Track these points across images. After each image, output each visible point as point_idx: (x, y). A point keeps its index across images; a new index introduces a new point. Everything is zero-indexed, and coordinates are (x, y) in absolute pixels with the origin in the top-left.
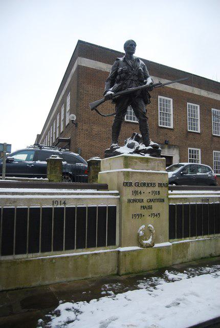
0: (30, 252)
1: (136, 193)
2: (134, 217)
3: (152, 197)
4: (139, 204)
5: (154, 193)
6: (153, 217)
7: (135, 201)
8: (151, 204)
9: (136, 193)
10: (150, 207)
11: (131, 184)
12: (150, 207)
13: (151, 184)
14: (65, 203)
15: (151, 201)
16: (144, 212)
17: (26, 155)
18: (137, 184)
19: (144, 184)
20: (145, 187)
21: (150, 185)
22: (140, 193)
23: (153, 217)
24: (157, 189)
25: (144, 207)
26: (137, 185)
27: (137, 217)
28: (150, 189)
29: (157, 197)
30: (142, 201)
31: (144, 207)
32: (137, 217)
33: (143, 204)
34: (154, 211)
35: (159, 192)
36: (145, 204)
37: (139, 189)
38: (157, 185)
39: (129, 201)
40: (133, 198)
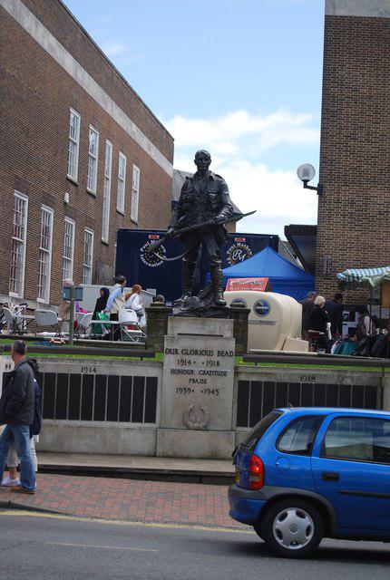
0: (57, 418)
1: (182, 362)
4: (189, 377)
5: (212, 363)
7: (180, 372)
8: (204, 377)
10: (204, 382)
11: (176, 352)
12: (204, 382)
13: (206, 352)
15: (205, 373)
16: (192, 386)
19: (196, 352)
22: (189, 362)
24: (215, 358)
25: (194, 381)
26: (185, 352)
29: (214, 368)
31: (194, 381)
33: (193, 377)
35: (218, 363)
37: (185, 357)
38: (215, 353)
39: (173, 371)
40: (179, 367)
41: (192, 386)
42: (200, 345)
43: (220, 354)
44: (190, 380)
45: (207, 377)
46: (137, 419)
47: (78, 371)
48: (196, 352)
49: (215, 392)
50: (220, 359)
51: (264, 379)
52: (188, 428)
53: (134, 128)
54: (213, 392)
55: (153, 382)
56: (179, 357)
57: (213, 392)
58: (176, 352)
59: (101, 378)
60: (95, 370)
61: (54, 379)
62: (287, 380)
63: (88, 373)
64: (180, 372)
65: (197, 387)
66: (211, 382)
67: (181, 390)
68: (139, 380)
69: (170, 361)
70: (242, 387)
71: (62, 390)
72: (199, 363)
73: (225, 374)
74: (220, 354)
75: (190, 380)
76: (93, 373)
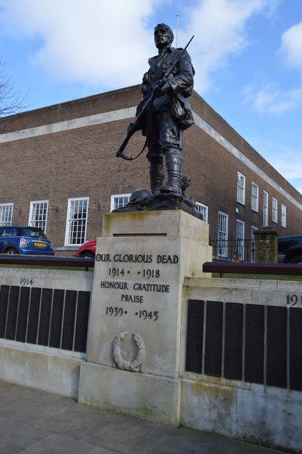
2: (110, 313)
3: (144, 282)
4: (122, 292)
5: (149, 273)
6: (143, 317)
7: (111, 285)
8: (140, 293)
11: (107, 258)
12: (139, 299)
13: (143, 257)
14: (31, 282)
15: (140, 287)
16: (126, 305)
17: (276, 222)
18: (117, 258)
19: (130, 258)
20: (132, 263)
21: (140, 259)
22: (122, 272)
23: (143, 317)
24: (154, 266)
25: (127, 298)
26: (118, 258)
27: (115, 313)
28: (139, 267)
30: (125, 286)
31: (127, 298)
32: (115, 313)
35: (158, 272)
36: (131, 292)
37: (120, 266)
38: (154, 259)
39: (103, 285)
40: (111, 280)
42: (132, 246)
43: (161, 259)
44: (123, 296)
45: (142, 293)
46: (67, 347)
47: (18, 283)
48: (130, 258)
50: (161, 267)
51: (226, 299)
52: (117, 366)
53: (281, 189)
54: (150, 315)
55: (86, 297)
56: (111, 265)
57: (150, 315)
58: (107, 258)
59: (37, 290)
60: (31, 282)
61: (18, 290)
62: (261, 301)
63: (26, 285)
64: (111, 285)
66: (150, 300)
67: (113, 311)
68: (72, 294)
69: (101, 268)
70: (194, 308)
71: (35, 302)
74: (161, 259)
75: (123, 296)
76: (29, 286)
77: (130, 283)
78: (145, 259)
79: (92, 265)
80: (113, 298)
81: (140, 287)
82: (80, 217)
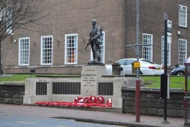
1: (85, 78)
4: (86, 82)
7: (85, 81)
9: (85, 78)
10: (90, 83)
11: (84, 75)
12: (90, 83)
15: (90, 81)
16: (87, 84)
19: (88, 75)
25: (88, 83)
26: (86, 75)
29: (92, 79)
31: (88, 83)
34: (91, 84)
38: (92, 75)
39: (83, 81)
41: (87, 84)
42: (89, 73)
43: (93, 75)
45: (90, 82)
48: (88, 75)
49: (92, 86)
55: (80, 83)
56: (84, 77)
58: (84, 75)
64: (85, 81)
65: (88, 85)
66: (92, 83)
67: (86, 85)
68: (77, 83)
70: (99, 84)
72: (89, 78)
73: (94, 81)
74: (93, 75)
77: (88, 80)
78: (91, 75)
79: (80, 77)
80: (85, 83)
81: (90, 81)
82: (48, 47)
